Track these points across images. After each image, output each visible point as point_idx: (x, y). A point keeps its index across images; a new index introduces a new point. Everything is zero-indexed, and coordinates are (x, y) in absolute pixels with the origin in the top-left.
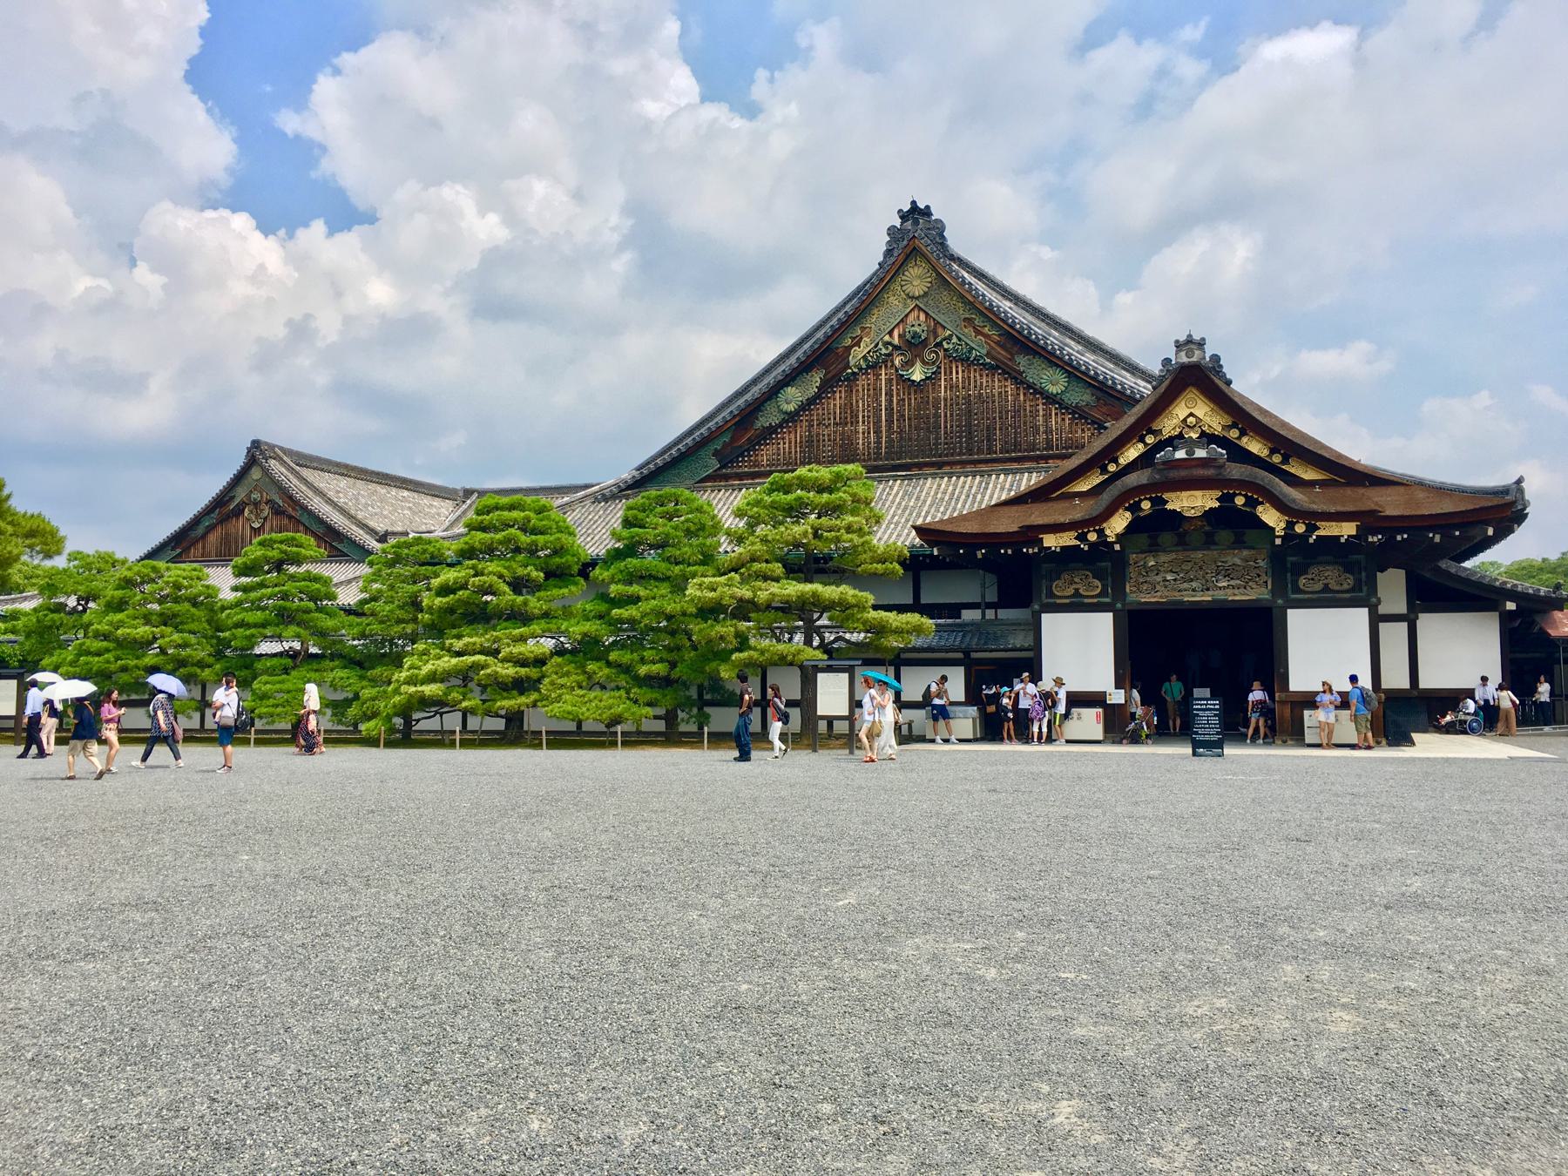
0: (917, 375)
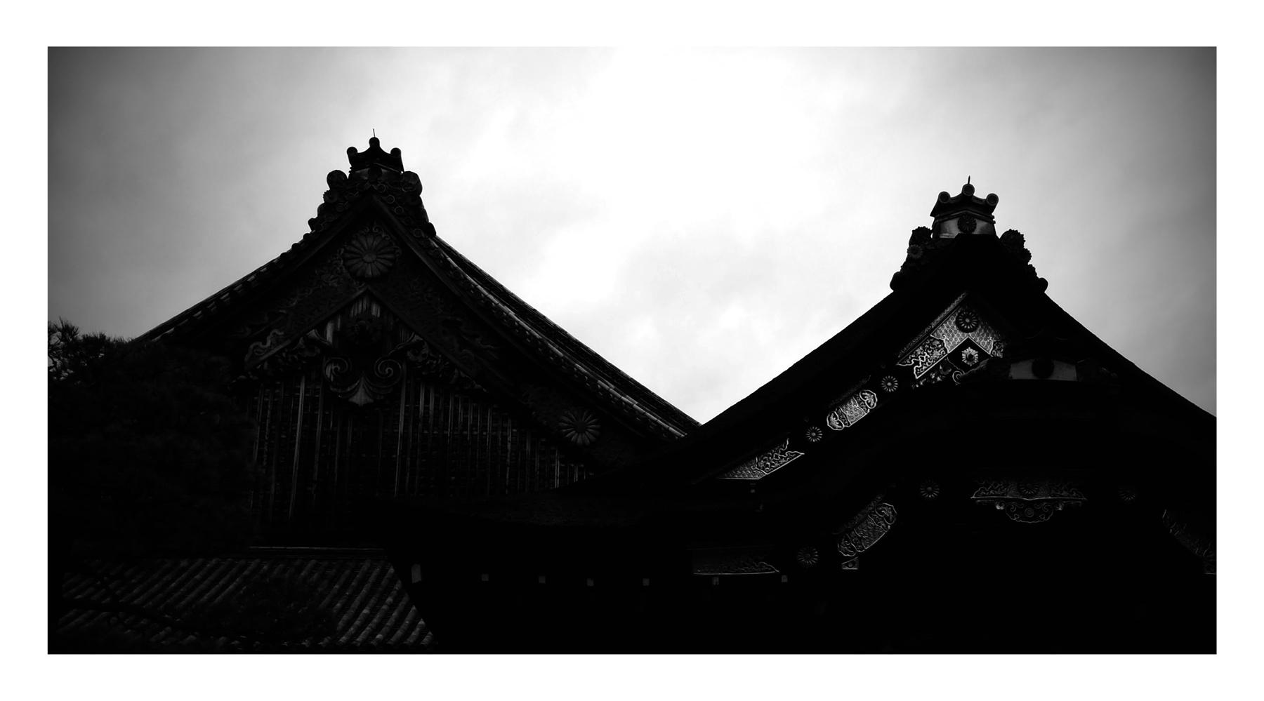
0: (360, 398)
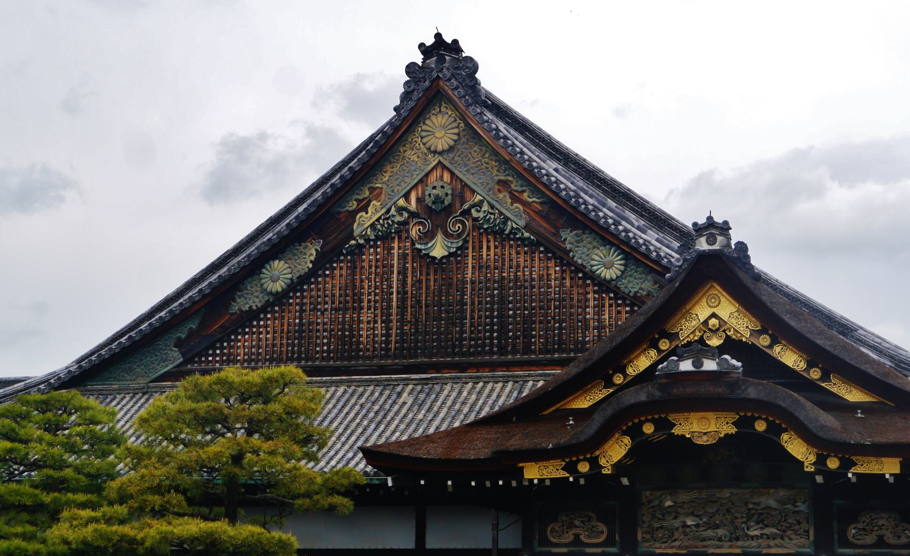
0: (438, 249)
